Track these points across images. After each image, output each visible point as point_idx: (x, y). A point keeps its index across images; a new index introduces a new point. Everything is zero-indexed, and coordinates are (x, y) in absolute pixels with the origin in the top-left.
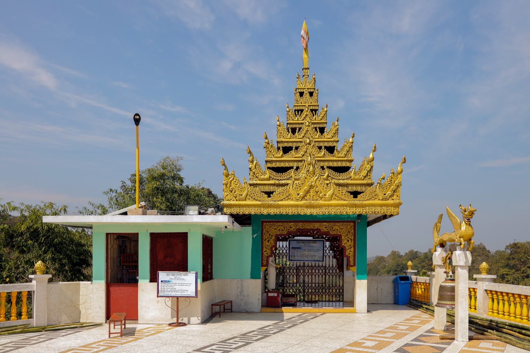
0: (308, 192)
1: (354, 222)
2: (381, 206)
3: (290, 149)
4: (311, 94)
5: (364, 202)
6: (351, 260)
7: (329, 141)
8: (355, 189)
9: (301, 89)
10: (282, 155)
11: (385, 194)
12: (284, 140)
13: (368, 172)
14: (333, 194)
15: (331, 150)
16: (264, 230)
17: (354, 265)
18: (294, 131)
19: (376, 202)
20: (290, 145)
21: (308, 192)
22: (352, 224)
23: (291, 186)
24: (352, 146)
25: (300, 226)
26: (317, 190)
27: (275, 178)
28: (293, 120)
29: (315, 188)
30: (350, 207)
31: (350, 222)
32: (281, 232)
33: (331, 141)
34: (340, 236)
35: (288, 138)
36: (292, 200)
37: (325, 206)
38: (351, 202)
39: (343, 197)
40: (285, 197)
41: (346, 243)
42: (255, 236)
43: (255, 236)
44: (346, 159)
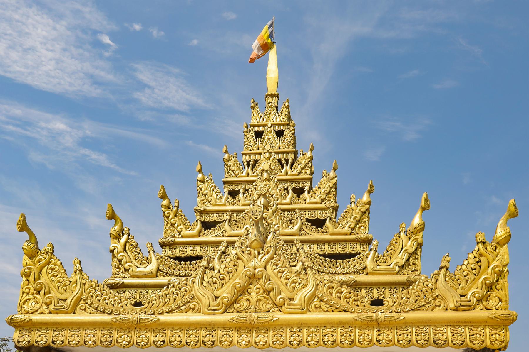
0: (243, 291)
2: (454, 324)
5: (403, 315)
7: (315, 209)
9: (259, 126)
10: (200, 232)
11: (462, 296)
13: (410, 255)
14: (314, 295)
19: (439, 314)
21: (243, 291)
24: (368, 210)
26: (268, 286)
27: (171, 271)
28: (236, 176)
29: (262, 281)
30: (360, 328)
33: (320, 209)
35: (220, 201)
36: (199, 311)
37: (289, 325)
38: (363, 315)
39: (342, 303)
40: (179, 302)
44: (353, 237)
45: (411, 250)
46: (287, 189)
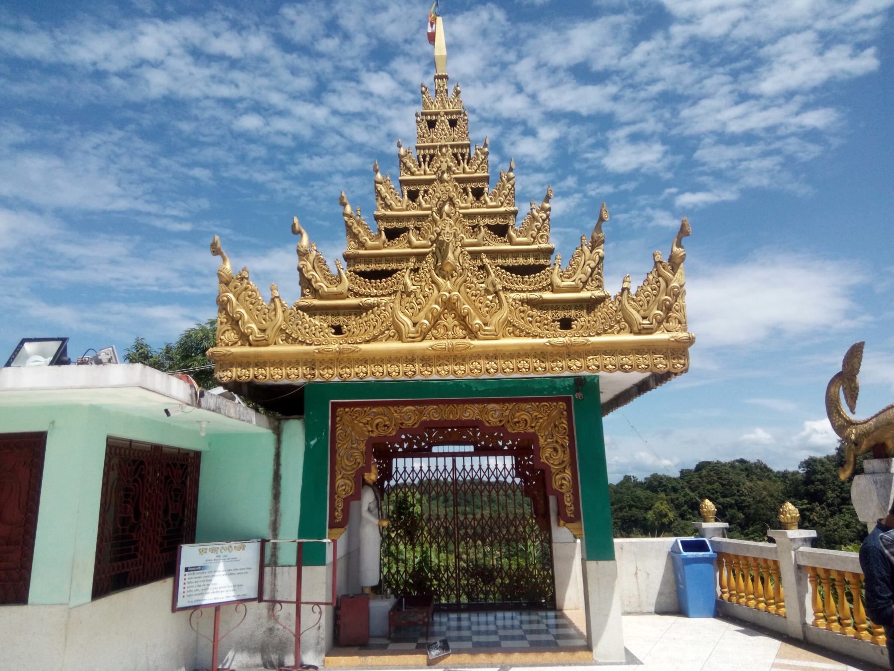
1: (567, 401)
3: (406, 230)
4: (453, 123)
6: (568, 501)
8: (562, 314)
10: (384, 242)
12: (389, 213)
15: (501, 231)
16: (339, 427)
17: (576, 518)
18: (413, 196)
20: (405, 224)
22: (562, 405)
23: (398, 301)
25: (432, 413)
28: (413, 174)
31: (557, 400)
32: (382, 432)
34: (533, 438)
35: (401, 206)
41: (551, 455)
42: (312, 443)
43: (312, 443)
45: (593, 264)
46: (465, 190)
